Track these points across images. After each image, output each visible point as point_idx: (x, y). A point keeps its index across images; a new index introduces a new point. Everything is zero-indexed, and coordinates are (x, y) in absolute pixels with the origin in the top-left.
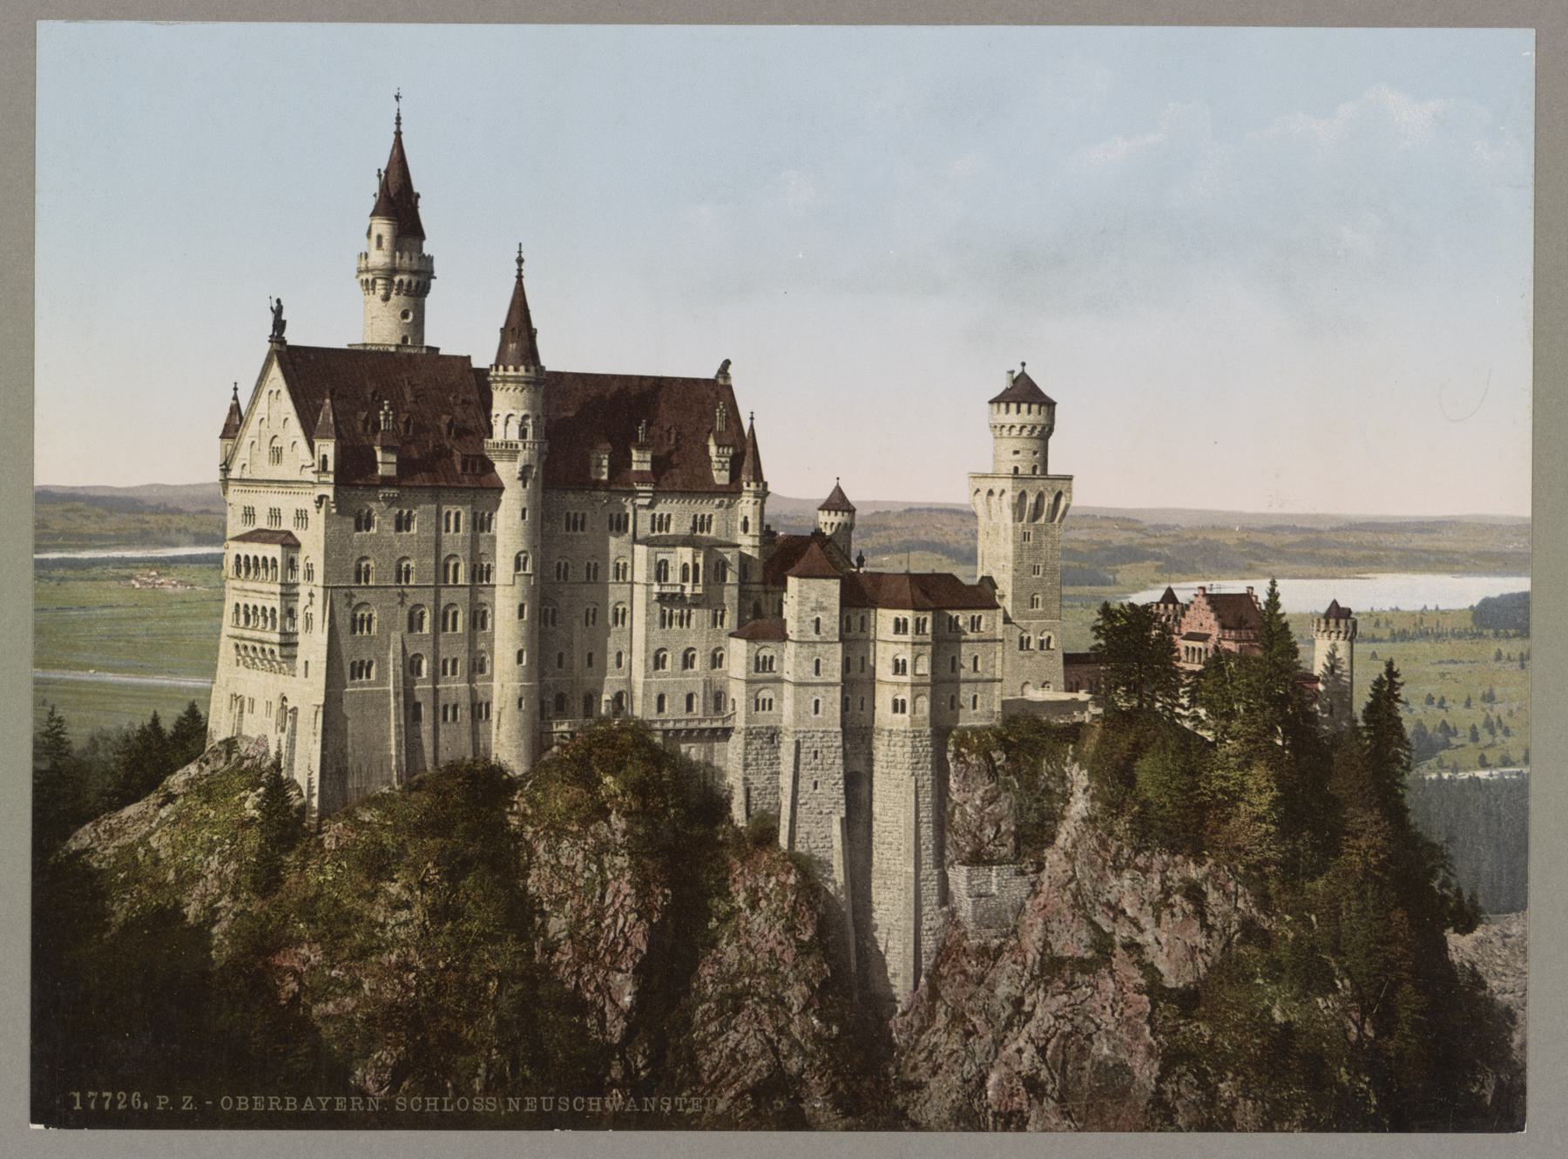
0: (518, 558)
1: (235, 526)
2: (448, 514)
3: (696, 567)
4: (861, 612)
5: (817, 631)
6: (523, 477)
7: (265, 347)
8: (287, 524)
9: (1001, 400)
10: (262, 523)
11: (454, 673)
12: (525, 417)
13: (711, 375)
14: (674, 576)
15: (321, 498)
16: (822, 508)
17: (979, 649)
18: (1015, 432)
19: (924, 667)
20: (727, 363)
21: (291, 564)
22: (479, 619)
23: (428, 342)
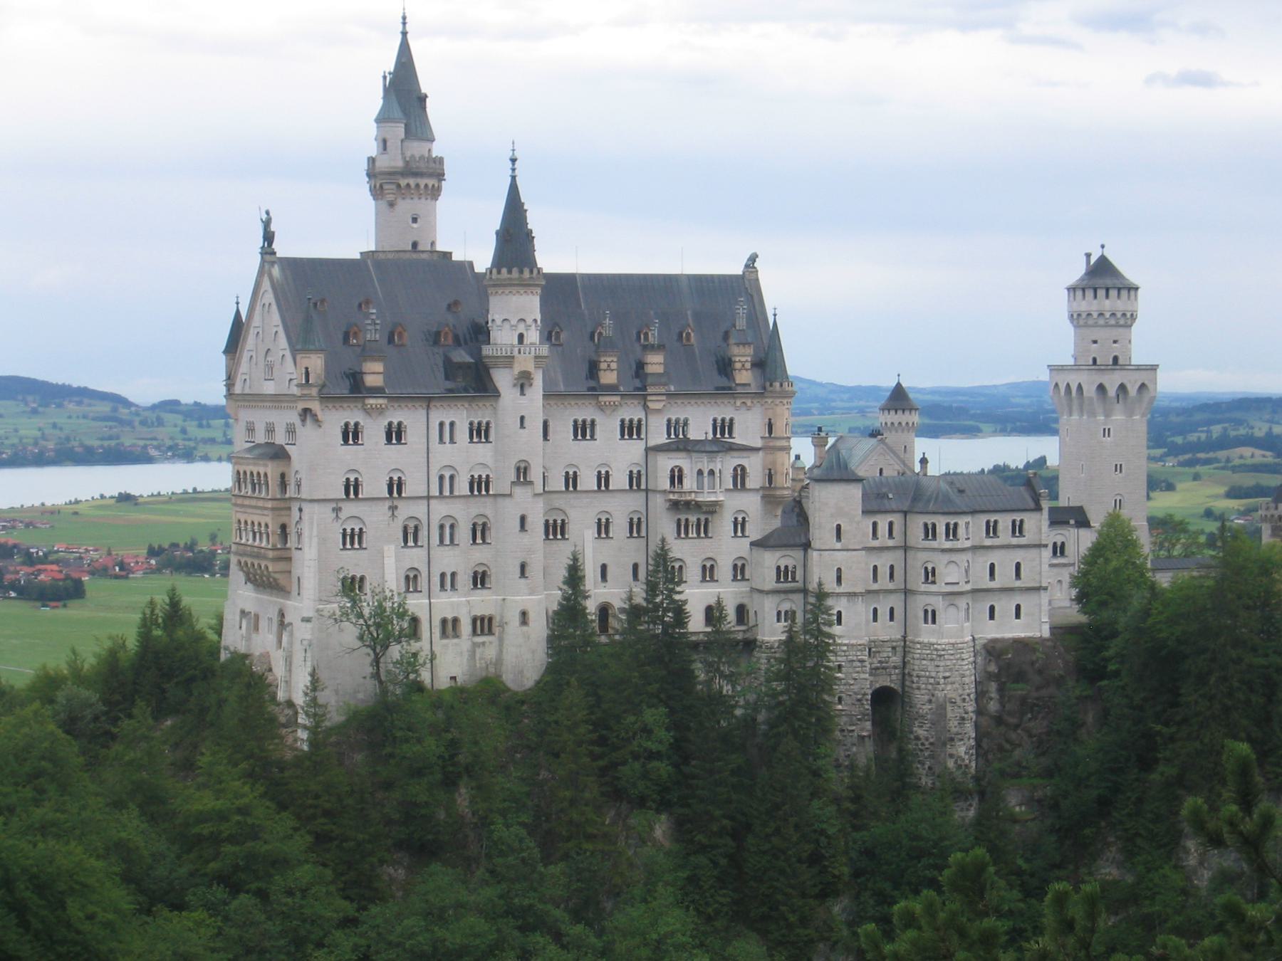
0: (518, 469)
3: (712, 472)
4: (890, 518)
6: (523, 382)
8: (280, 438)
10: (261, 438)
12: (522, 320)
13: (738, 269)
14: (689, 483)
15: (306, 412)
17: (1018, 556)
18: (1090, 322)
20: (753, 258)
22: (480, 532)
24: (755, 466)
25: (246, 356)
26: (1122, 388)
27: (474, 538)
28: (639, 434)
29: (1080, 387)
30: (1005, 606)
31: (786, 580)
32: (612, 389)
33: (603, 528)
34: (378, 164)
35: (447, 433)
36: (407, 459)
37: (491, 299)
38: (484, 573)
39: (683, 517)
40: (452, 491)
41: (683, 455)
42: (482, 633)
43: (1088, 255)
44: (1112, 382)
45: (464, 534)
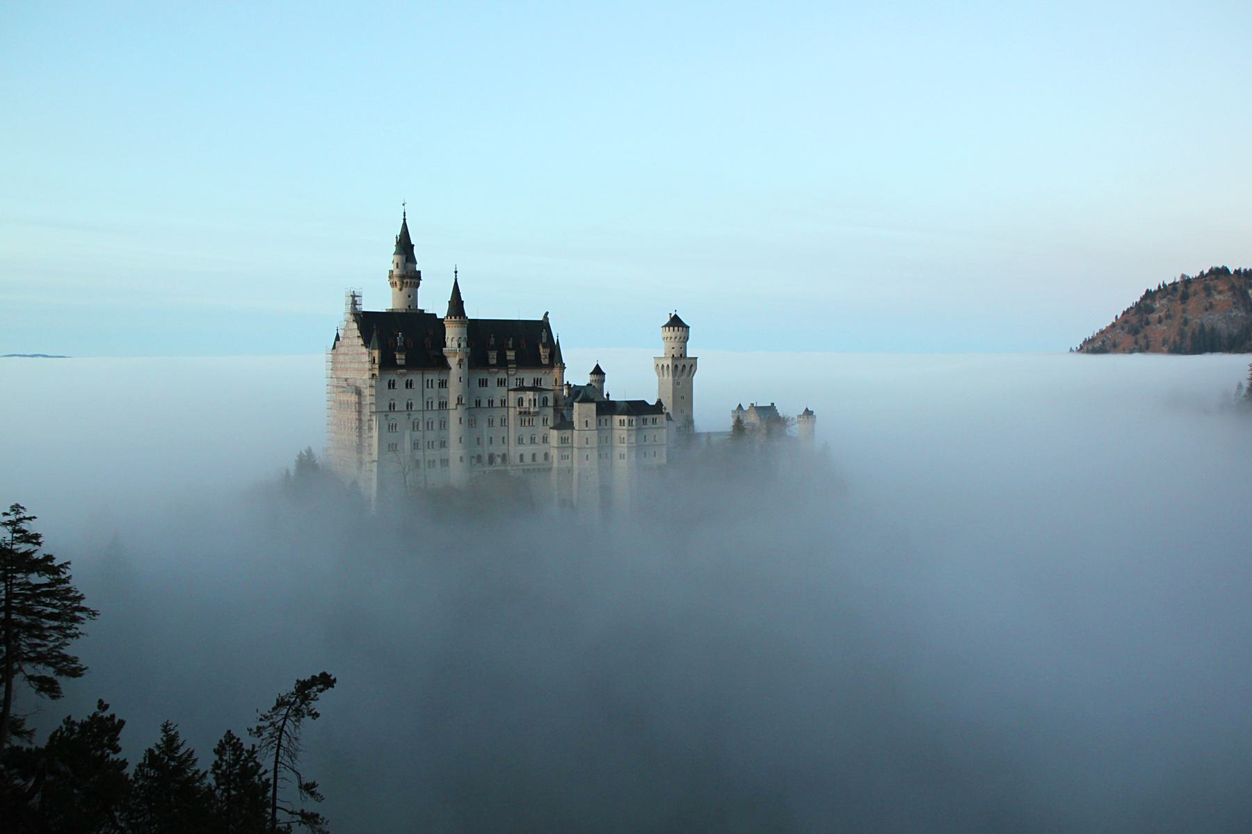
6: (460, 362)
9: (668, 325)
13: (541, 319)
14: (526, 404)
19: (633, 439)
22: (443, 425)
24: (550, 396)
32: (493, 366)
33: (491, 423)
35: (430, 384)
36: (414, 395)
44: (680, 363)
45: (436, 426)
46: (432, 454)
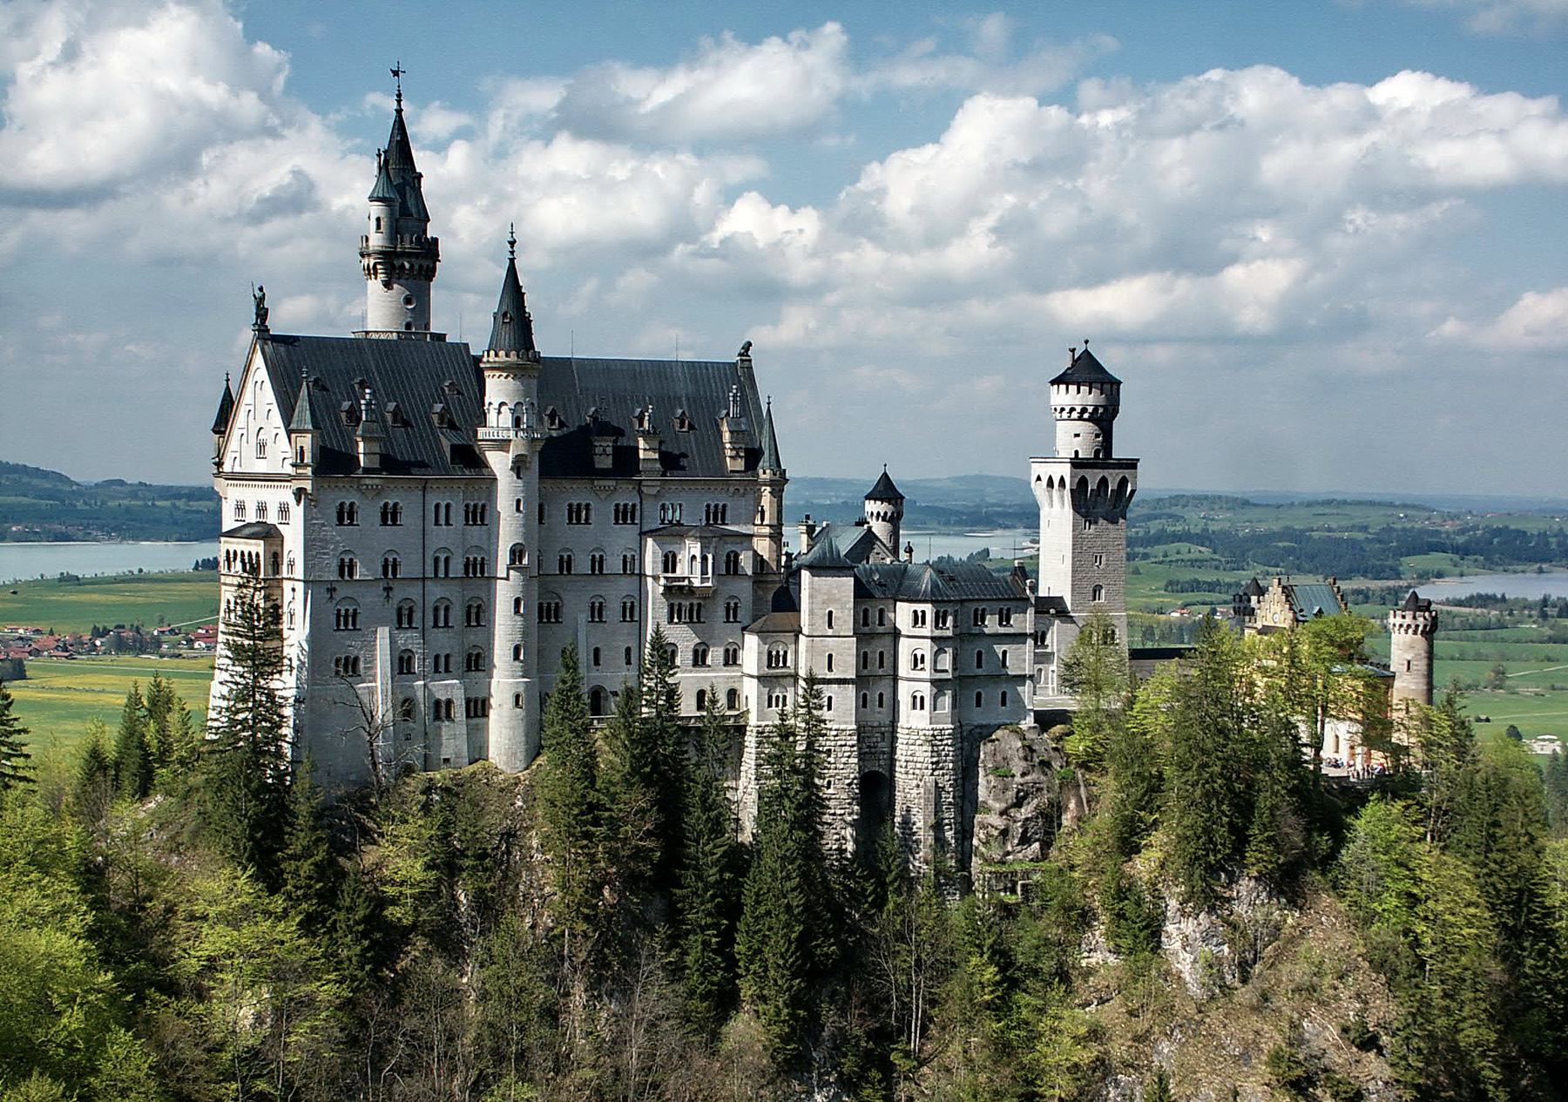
0: (513, 552)
1: (229, 523)
2: (437, 506)
3: (704, 558)
5: (830, 626)
6: (518, 467)
7: (248, 335)
8: (272, 518)
10: (251, 516)
11: (447, 670)
14: (682, 570)
15: (299, 493)
16: (868, 497)
19: (946, 661)
21: (276, 560)
23: (435, 328)
25: (236, 434)
26: (1104, 482)
27: (469, 621)
28: (633, 519)
29: (1062, 479)
30: (992, 694)
31: (777, 666)
32: (605, 474)
33: (597, 612)
34: (371, 243)
35: (442, 516)
36: (403, 541)
37: (488, 381)
38: (478, 655)
39: (676, 602)
40: (447, 573)
41: (677, 539)
42: (476, 716)
43: (1073, 351)
45: (457, 615)
46: (450, 688)
